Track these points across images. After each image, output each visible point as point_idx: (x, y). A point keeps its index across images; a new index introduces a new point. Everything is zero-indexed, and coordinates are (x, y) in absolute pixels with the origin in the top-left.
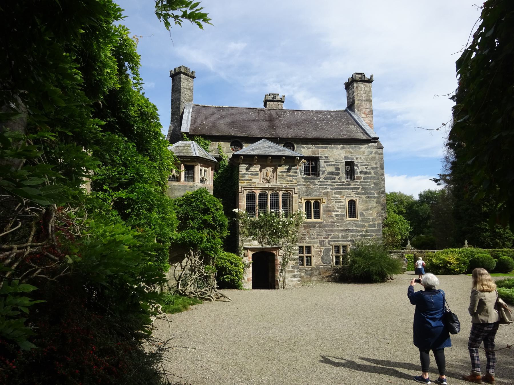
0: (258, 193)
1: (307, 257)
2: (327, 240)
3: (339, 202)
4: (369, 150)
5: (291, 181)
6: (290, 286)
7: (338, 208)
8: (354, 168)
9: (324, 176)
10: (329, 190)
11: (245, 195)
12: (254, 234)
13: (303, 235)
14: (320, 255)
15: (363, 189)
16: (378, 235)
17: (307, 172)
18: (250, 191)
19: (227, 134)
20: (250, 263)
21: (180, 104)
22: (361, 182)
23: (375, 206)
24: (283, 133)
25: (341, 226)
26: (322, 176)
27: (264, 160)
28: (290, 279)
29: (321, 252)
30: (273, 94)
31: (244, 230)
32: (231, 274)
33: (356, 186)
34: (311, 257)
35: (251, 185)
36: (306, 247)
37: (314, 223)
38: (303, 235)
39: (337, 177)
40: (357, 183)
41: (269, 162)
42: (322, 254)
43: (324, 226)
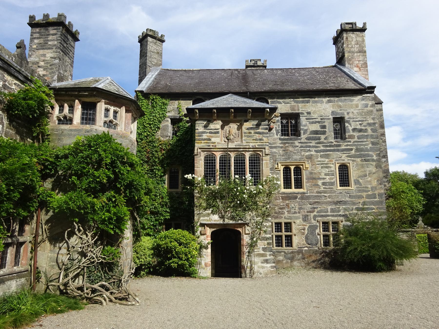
0: (218, 155)
1: (286, 236)
2: (312, 215)
3: (327, 167)
4: (363, 102)
5: (260, 140)
6: (261, 274)
7: (326, 175)
8: (345, 125)
9: (306, 136)
10: (313, 153)
11: (202, 158)
12: (214, 206)
13: (281, 209)
14: (303, 234)
15: (357, 150)
16: (380, 208)
17: (284, 131)
18: (209, 153)
19: (188, 90)
20: (208, 243)
21: (146, 68)
22: (354, 142)
23: (374, 171)
24: (254, 87)
25: (329, 197)
26: (303, 137)
27: (226, 115)
28: (260, 264)
29: (304, 229)
30: (254, 60)
31: (201, 201)
32: (179, 258)
33: (349, 147)
34: (291, 236)
35: (209, 146)
36: (286, 223)
37: (295, 193)
38: (281, 209)
39: (323, 137)
40: (349, 143)
41: (232, 118)
42: (306, 232)
43: (308, 198)
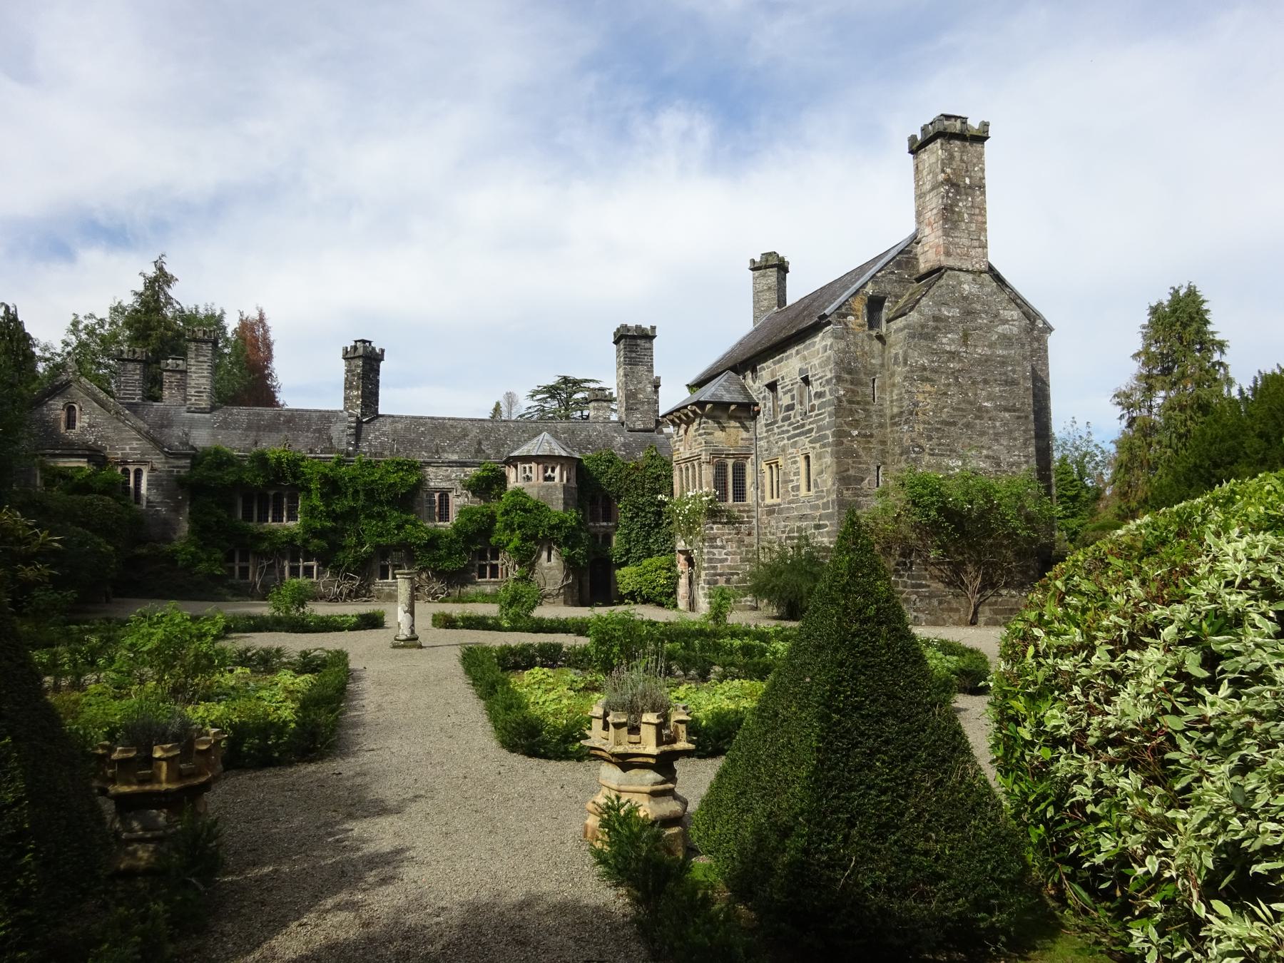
39: (792, 413)
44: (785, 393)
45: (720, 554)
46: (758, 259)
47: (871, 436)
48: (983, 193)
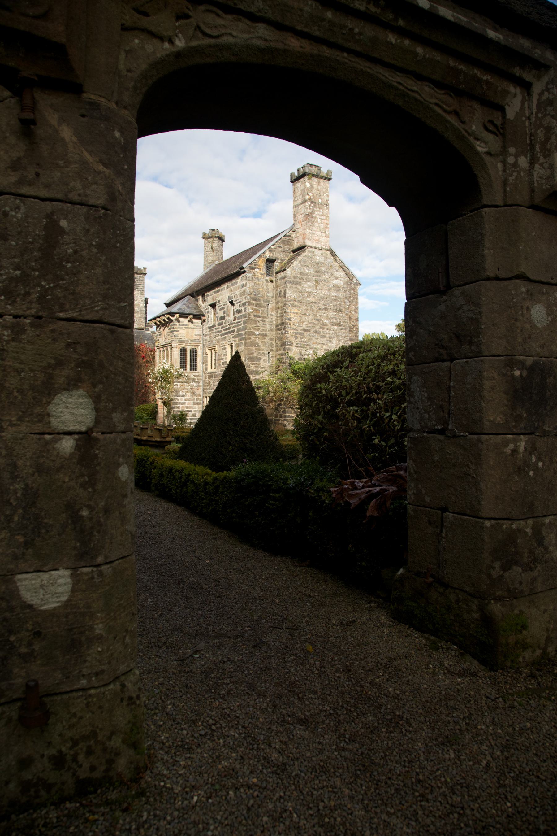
39: (224, 321)
44: (220, 310)
45: (182, 400)
46: (207, 232)
47: (266, 335)
48: (328, 208)
